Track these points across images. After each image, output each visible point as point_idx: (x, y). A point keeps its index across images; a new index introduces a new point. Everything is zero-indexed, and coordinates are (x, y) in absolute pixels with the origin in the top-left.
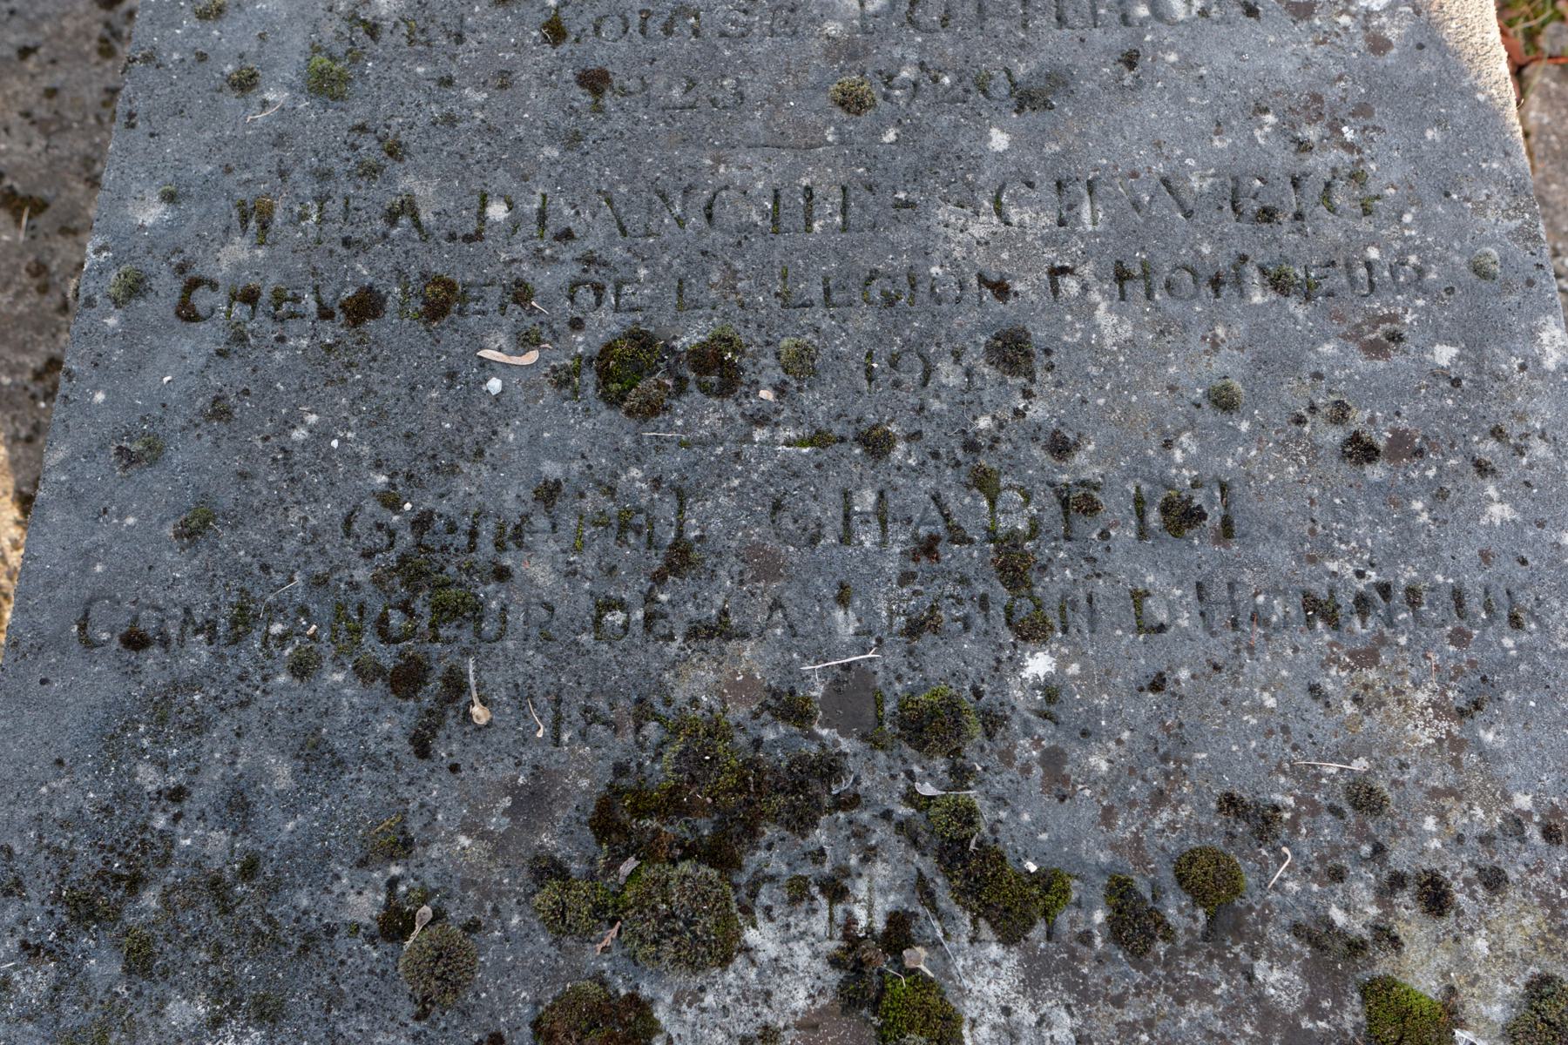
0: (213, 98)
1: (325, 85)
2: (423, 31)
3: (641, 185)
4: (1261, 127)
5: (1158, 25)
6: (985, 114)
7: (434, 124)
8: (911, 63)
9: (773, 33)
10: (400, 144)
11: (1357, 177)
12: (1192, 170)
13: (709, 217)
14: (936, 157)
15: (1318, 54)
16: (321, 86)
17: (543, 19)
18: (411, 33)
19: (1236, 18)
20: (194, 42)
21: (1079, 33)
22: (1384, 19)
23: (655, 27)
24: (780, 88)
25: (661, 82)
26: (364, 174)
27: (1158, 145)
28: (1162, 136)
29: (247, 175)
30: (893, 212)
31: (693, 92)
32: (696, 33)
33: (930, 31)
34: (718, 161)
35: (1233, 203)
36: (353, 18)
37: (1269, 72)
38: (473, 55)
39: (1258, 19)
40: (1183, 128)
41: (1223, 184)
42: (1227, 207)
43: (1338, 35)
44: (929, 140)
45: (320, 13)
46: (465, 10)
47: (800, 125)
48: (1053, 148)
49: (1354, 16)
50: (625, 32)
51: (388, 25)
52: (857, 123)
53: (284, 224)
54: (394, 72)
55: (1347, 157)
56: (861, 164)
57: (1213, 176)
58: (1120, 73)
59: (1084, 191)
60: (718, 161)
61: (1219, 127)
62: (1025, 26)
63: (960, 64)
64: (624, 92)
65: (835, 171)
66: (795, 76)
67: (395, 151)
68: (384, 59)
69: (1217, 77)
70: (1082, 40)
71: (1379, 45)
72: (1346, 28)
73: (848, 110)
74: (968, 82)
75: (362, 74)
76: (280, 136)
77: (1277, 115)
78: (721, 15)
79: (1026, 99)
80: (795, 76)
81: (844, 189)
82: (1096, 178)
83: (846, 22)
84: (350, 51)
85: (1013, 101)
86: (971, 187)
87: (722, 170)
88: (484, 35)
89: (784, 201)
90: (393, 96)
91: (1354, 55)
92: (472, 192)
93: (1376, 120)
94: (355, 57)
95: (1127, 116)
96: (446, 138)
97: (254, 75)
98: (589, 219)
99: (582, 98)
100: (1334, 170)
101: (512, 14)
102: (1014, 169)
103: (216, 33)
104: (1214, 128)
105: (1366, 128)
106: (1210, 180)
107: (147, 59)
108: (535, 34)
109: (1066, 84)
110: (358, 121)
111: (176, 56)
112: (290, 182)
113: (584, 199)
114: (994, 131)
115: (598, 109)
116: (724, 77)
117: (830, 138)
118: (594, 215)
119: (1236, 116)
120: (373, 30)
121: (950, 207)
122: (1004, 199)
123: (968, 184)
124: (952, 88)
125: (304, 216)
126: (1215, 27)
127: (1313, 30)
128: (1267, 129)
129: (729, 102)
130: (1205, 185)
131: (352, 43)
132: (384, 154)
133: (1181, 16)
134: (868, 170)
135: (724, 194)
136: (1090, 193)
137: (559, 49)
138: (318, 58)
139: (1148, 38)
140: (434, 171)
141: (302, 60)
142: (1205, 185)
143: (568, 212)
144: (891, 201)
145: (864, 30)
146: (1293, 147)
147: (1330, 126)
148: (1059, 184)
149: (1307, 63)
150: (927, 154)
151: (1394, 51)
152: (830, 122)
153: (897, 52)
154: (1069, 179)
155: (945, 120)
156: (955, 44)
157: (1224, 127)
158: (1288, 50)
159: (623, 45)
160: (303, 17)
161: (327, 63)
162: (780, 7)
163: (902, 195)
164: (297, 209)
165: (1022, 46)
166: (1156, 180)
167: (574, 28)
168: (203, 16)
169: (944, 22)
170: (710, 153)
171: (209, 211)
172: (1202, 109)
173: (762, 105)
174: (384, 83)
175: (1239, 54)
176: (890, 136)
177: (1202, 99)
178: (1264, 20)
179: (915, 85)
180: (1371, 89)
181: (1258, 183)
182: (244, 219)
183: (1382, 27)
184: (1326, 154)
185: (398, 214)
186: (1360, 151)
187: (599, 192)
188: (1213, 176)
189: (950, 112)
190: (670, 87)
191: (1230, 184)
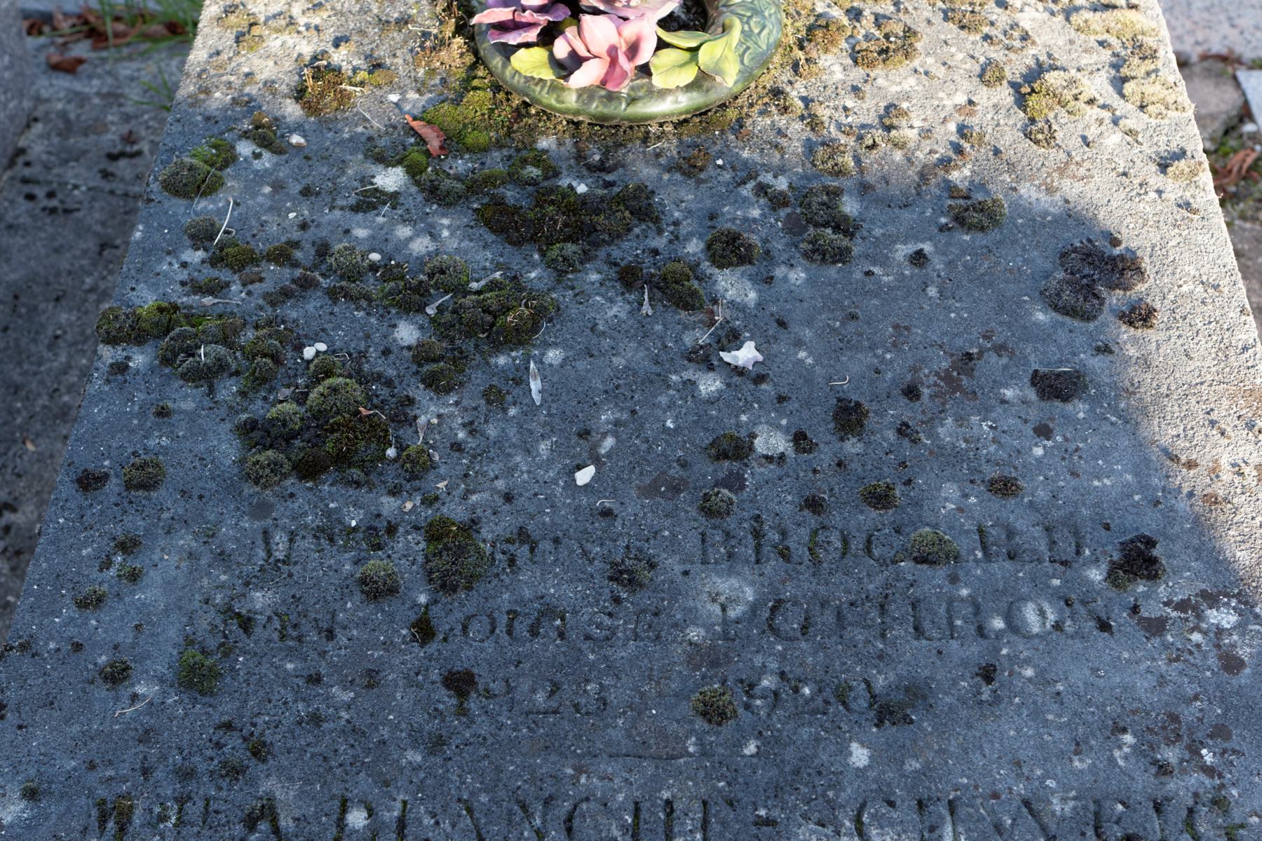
0: (84, 691)
1: (196, 678)
2: (295, 626)
3: (502, 794)
4: (1120, 748)
5: (1014, 638)
6: (845, 728)
7: (300, 723)
8: (772, 672)
9: (637, 637)
10: (264, 744)
11: (1219, 803)
12: (1053, 792)
13: (569, 830)
14: (797, 772)
15: (1172, 671)
16: (191, 681)
17: (414, 618)
18: (284, 627)
19: (1090, 633)
20: (72, 631)
21: (937, 644)
22: (1235, 637)
23: (521, 628)
24: (642, 695)
25: (525, 686)
26: (227, 775)
27: (1018, 764)
28: (1022, 755)
29: (110, 773)
30: (754, 830)
31: (556, 697)
32: (561, 635)
33: (791, 639)
34: (579, 770)
35: (1097, 828)
36: (228, 612)
37: (1125, 689)
38: (343, 652)
39: (1112, 634)
40: (1043, 746)
41: (1085, 808)
42: (1090, 832)
43: (1191, 653)
44: (789, 754)
45: (197, 604)
46: (338, 605)
47: (662, 734)
48: (913, 765)
49: (1205, 633)
50: (492, 632)
51: (261, 619)
52: (718, 734)
53: (142, 826)
54: (263, 669)
55: (1207, 781)
56: (723, 777)
57: (1075, 798)
58: (978, 687)
59: (945, 812)
60: (579, 770)
61: (1079, 747)
62: (883, 636)
63: (820, 674)
64: (489, 694)
65: (696, 784)
66: (658, 683)
67: (259, 751)
68: (256, 654)
69: (1074, 694)
70: (940, 652)
71: (1232, 664)
72: (1198, 646)
73: (710, 721)
74: (828, 693)
75: (232, 669)
76: (147, 732)
77: (1135, 736)
78: (586, 617)
79: (887, 712)
80: (658, 683)
81: (705, 803)
82: (957, 798)
83: (709, 628)
84: (223, 644)
85: (872, 713)
86: (832, 805)
87: (583, 780)
88: (355, 632)
89: (644, 815)
90: (261, 693)
91: (1208, 674)
92: (333, 797)
93: (1234, 743)
94: (227, 650)
95: (986, 733)
96: (310, 739)
97: (127, 668)
98: (449, 829)
99: (448, 701)
100: (1196, 795)
101: (383, 611)
102: (874, 786)
103: (94, 622)
104: (1073, 748)
105: (1225, 751)
106: (1072, 803)
107: (23, 647)
108: (404, 632)
109: (924, 698)
110: (226, 718)
111: (52, 645)
112: (152, 781)
113: (445, 808)
114: (854, 746)
115: (462, 711)
116: (587, 681)
117: (691, 749)
118: (453, 826)
119: (1094, 735)
120: (246, 624)
121: (812, 826)
122: (865, 818)
123: (829, 801)
124: (812, 699)
125: (163, 818)
126: (1070, 642)
127: (1166, 646)
128: (1126, 750)
129: (592, 708)
130: (1067, 809)
131: (225, 637)
132: (248, 754)
133: (1036, 630)
134: (729, 784)
135: (584, 806)
136: (952, 814)
137: (426, 648)
138: (191, 651)
139: (1004, 652)
140: (296, 773)
141: (175, 653)
142: (1067, 809)
143: (428, 821)
144: (751, 818)
145: (726, 637)
146: (1153, 770)
147: (1189, 747)
148: (920, 804)
149: (1162, 681)
150: (787, 769)
151: (1247, 671)
152: (692, 732)
153: (758, 660)
154: (930, 799)
155: (805, 733)
156: (815, 653)
157: (1083, 747)
158: (1143, 667)
159: (489, 646)
160: (180, 608)
161: (199, 657)
162: (644, 611)
163: (762, 812)
164: (157, 810)
165: (880, 657)
166: (1017, 802)
167: (442, 627)
168: (83, 604)
169: (804, 629)
170: (571, 762)
171: (68, 809)
172: (1060, 727)
173: (625, 713)
174: (253, 679)
175: (1095, 671)
176: (751, 749)
177: (1060, 716)
178: (1117, 635)
179: (776, 694)
180: (1226, 710)
181: (1120, 807)
182: (103, 819)
183: (1233, 646)
184: (1187, 778)
185: (258, 819)
186: (1220, 776)
187: (459, 800)
188: (1075, 798)
189: (810, 724)
190: (534, 691)
191: (1092, 807)
